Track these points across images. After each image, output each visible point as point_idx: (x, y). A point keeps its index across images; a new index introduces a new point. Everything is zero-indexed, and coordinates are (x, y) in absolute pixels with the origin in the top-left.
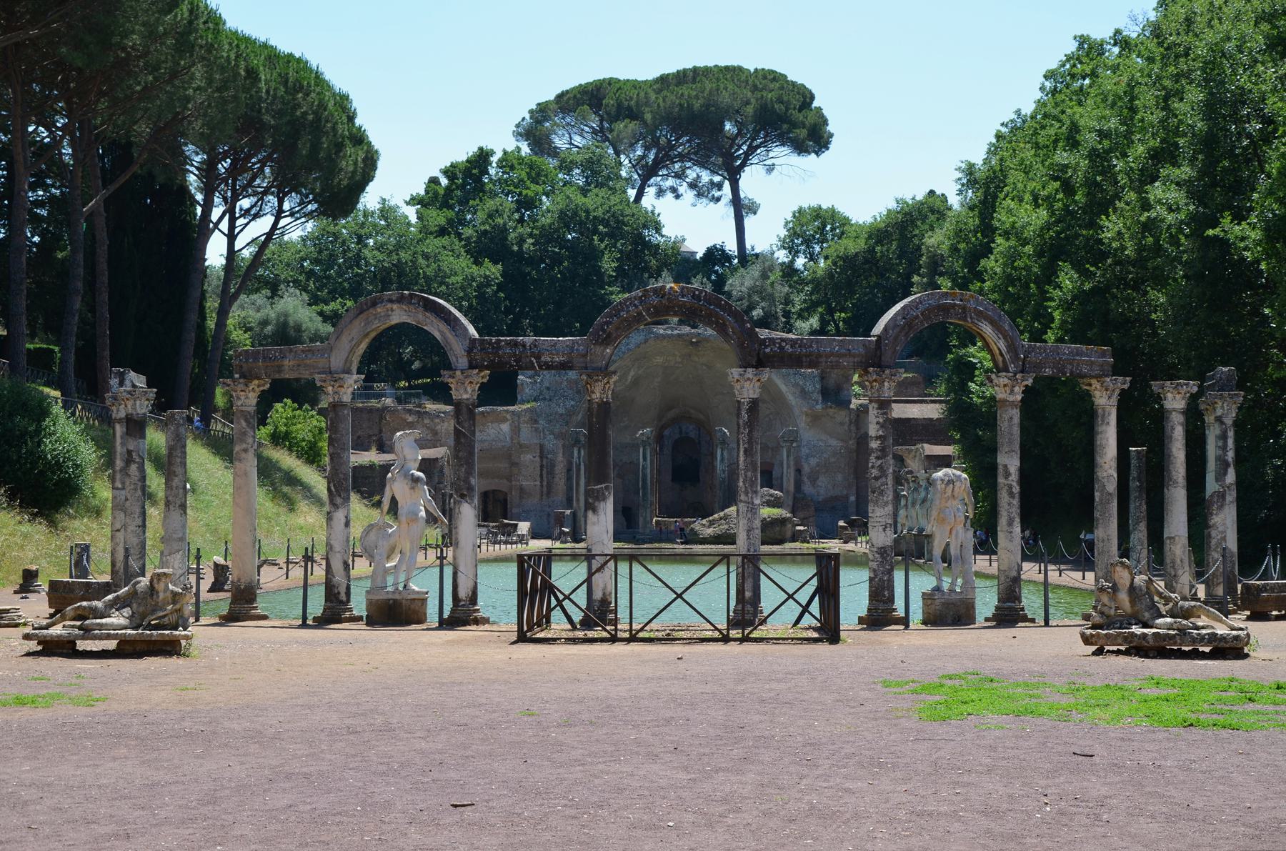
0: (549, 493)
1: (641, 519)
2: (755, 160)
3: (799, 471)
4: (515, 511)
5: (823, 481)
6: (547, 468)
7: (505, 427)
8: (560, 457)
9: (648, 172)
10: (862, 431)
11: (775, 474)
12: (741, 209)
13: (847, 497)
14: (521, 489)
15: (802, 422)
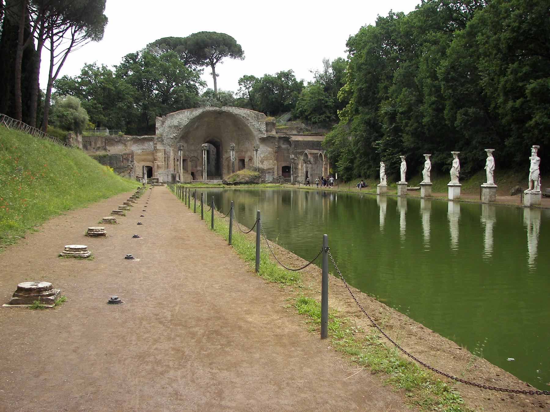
0: (168, 167)
5: (265, 163)
6: (167, 159)
7: (151, 143)
13: (274, 168)
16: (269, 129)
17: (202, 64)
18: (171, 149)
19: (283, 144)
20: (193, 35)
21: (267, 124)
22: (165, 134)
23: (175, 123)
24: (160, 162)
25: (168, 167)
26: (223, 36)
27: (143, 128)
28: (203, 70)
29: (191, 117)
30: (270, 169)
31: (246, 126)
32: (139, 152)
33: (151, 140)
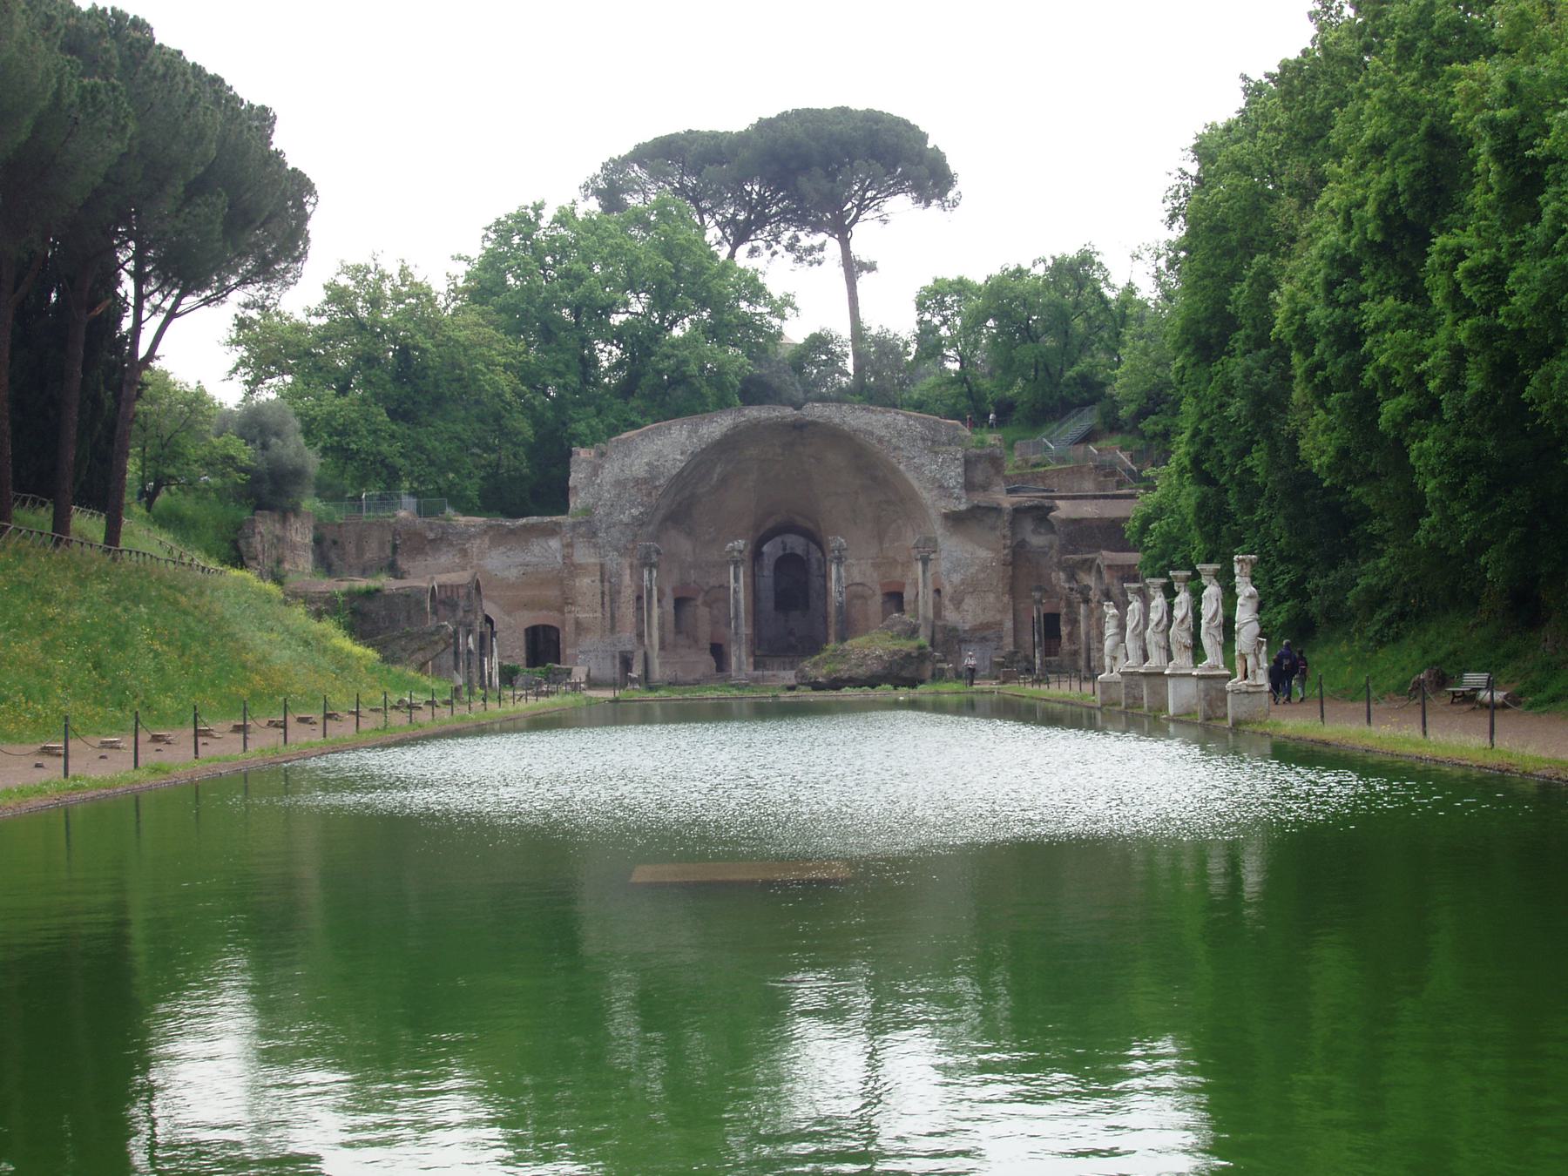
0: (613, 628)
1: (734, 660)
2: (868, 214)
3: (938, 591)
4: (569, 651)
5: (969, 603)
6: (610, 596)
7: (554, 544)
8: (627, 579)
9: (740, 234)
10: (1019, 537)
11: (908, 595)
12: (853, 269)
13: (1001, 623)
14: (578, 623)
15: (938, 529)
16: (979, 477)
17: (816, 228)
18: (626, 562)
19: (1035, 531)
20: (764, 125)
21: (969, 463)
22: (601, 511)
23: (638, 466)
24: (587, 610)
25: (613, 628)
26: (873, 119)
27: (531, 488)
28: (821, 248)
29: (694, 445)
30: (986, 626)
31: (895, 471)
32: (513, 574)
33: (551, 531)
